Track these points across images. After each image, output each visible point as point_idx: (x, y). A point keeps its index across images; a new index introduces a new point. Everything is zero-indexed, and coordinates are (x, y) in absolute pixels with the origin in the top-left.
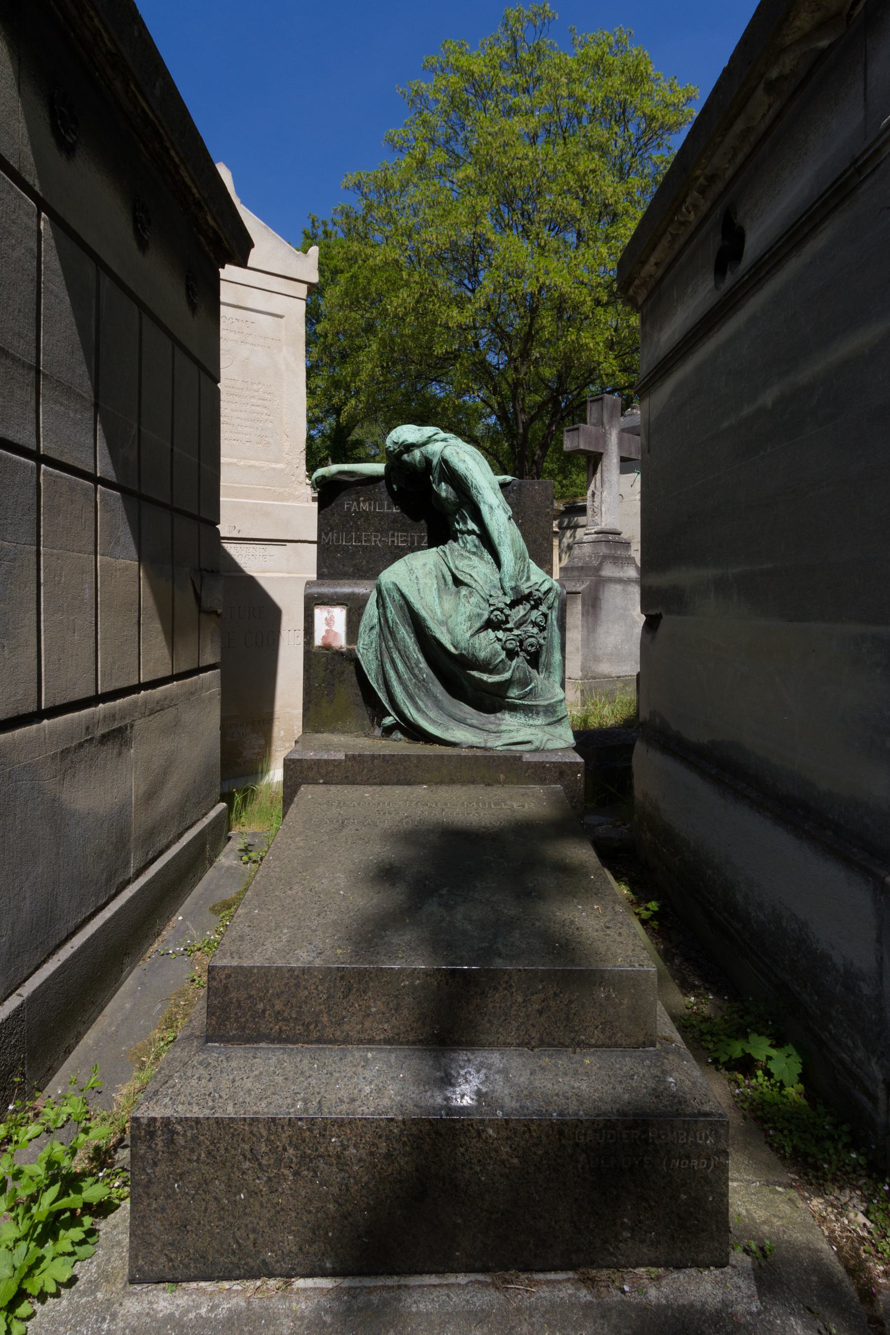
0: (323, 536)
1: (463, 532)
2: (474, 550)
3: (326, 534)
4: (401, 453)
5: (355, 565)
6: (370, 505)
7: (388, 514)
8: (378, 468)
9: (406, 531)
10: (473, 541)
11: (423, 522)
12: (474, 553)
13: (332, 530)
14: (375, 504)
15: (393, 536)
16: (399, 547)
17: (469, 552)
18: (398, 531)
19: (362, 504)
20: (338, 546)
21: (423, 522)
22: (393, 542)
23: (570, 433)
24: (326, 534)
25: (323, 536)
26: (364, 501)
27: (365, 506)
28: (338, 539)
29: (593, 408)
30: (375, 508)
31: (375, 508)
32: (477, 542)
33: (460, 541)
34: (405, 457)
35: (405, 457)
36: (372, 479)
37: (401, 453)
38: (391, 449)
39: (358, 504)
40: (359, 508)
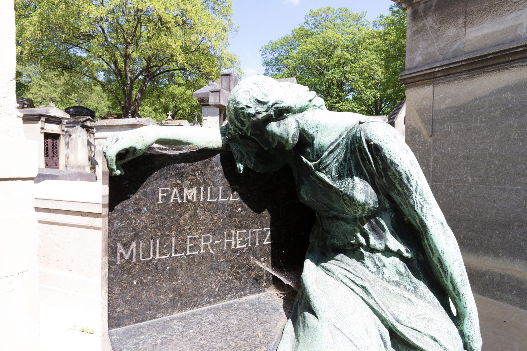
0: (121, 249)
1: (373, 250)
2: (397, 278)
3: (126, 246)
4: (268, 120)
5: (175, 290)
6: (199, 192)
7: (223, 204)
8: (208, 134)
9: (246, 228)
10: (396, 266)
11: (266, 212)
12: (397, 284)
13: (136, 237)
14: (205, 190)
15: (229, 236)
16: (236, 251)
17: (389, 282)
18: (236, 227)
19: (186, 191)
20: (148, 263)
21: (266, 212)
22: (229, 244)
23: (214, 93)
24: (126, 246)
25: (121, 249)
26: (190, 187)
27: (190, 193)
28: (147, 252)
29: (224, 80)
30: (205, 196)
31: (205, 196)
32: (402, 266)
33: (368, 261)
34: (273, 127)
35: (273, 127)
36: (205, 153)
37: (268, 120)
38: (252, 111)
39: (181, 192)
40: (182, 198)
